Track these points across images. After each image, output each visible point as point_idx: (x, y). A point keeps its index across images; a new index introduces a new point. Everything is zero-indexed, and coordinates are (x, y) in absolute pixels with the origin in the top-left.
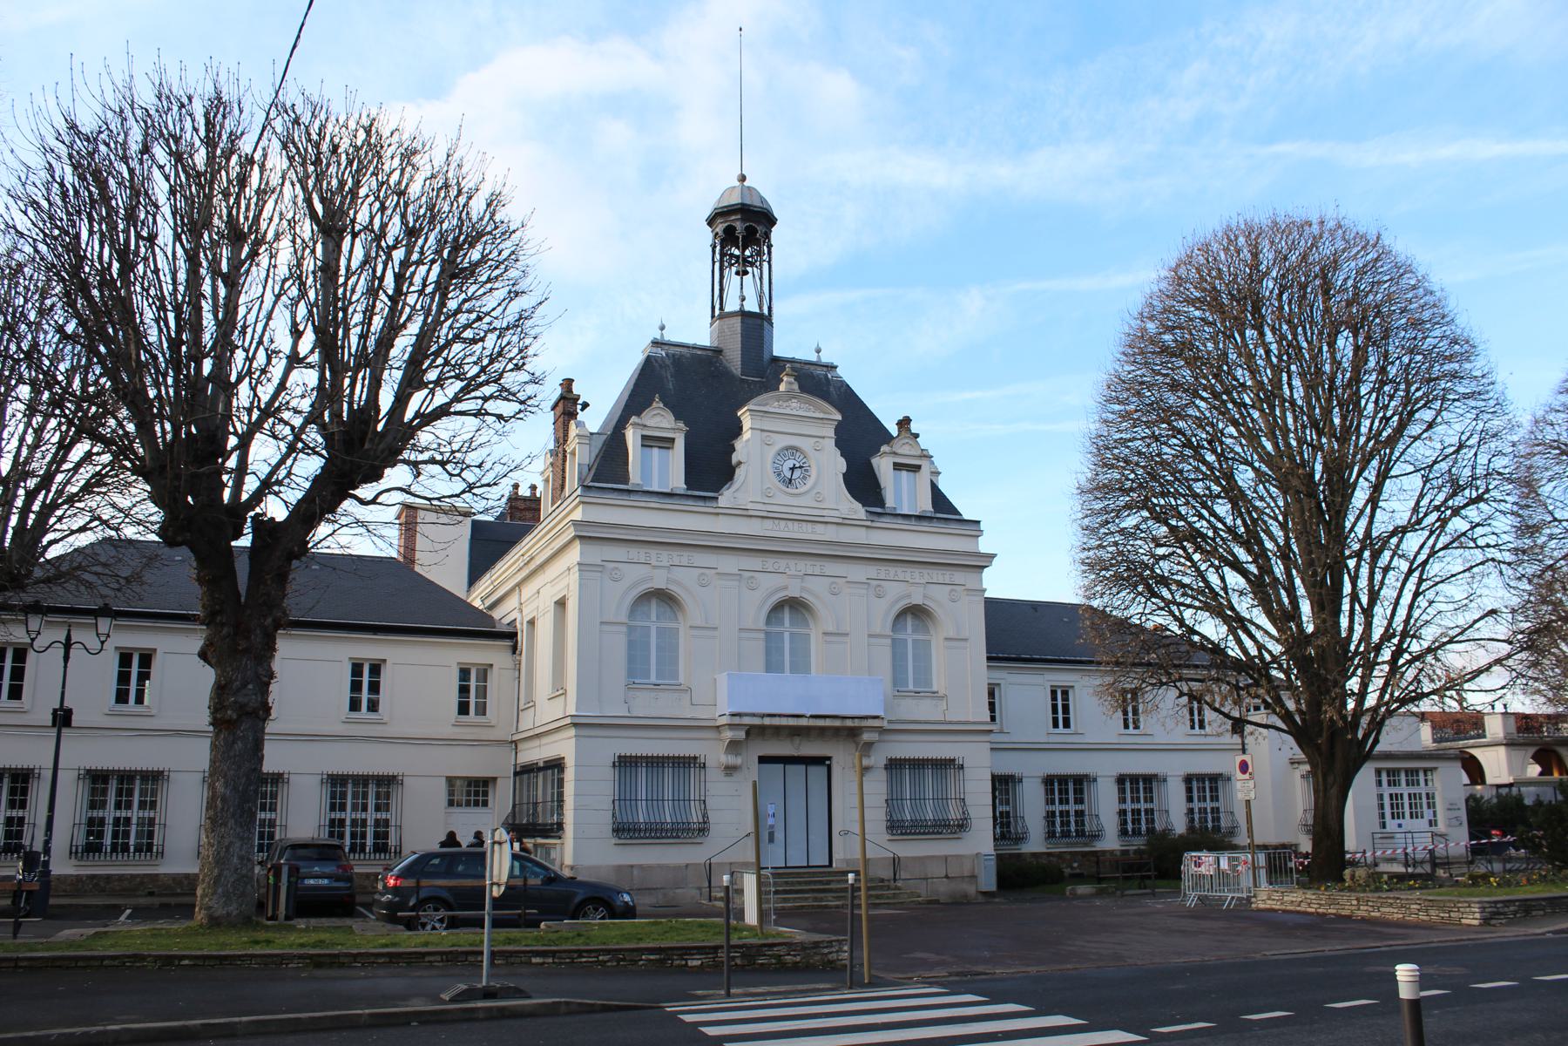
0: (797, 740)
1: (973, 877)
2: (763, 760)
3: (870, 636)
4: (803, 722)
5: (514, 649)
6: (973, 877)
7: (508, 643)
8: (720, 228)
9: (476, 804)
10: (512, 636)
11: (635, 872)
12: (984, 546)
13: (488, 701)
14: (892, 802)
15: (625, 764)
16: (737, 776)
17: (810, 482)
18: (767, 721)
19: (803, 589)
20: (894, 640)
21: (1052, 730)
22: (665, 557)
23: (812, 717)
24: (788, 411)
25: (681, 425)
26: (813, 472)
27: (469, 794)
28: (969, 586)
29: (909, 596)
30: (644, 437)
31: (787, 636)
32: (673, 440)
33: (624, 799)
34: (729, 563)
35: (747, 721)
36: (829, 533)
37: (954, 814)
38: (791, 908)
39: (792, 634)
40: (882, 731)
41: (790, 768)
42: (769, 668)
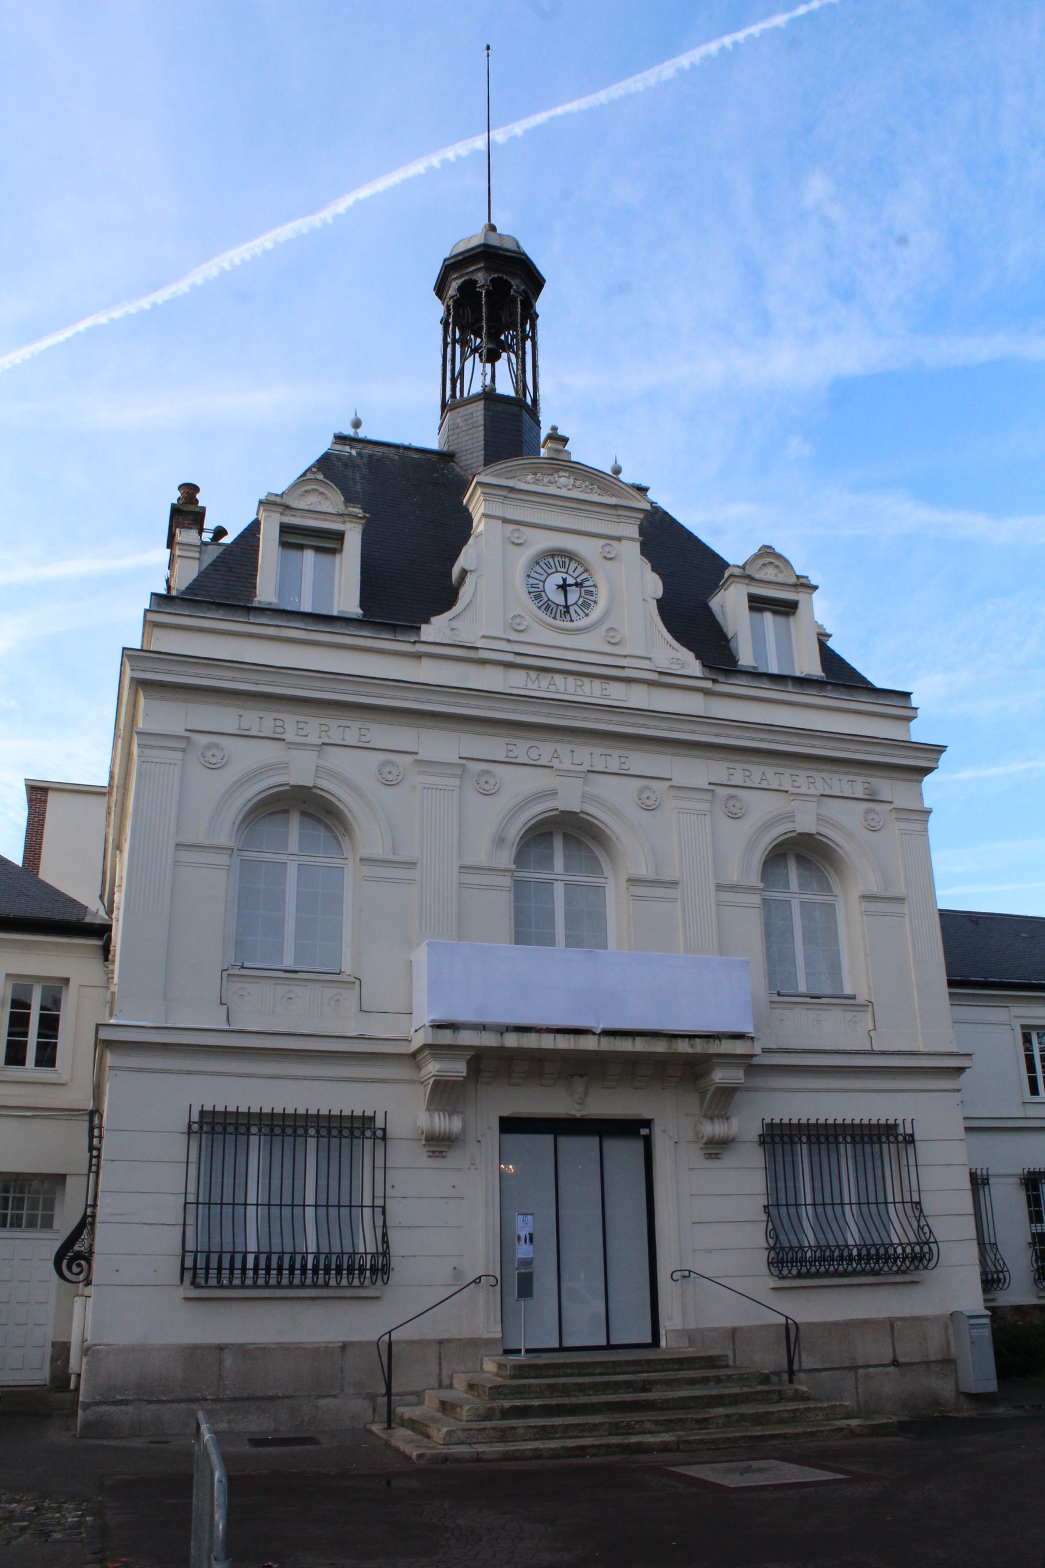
0: (579, 1085)
1: (948, 1362)
2: (510, 1125)
3: (720, 887)
4: (589, 1044)
5: (106, 952)
6: (948, 1362)
8: (452, 290)
9: (32, 1224)
10: (102, 931)
11: (228, 1362)
12: (919, 732)
13: (59, 1041)
14: (777, 1208)
15: (217, 1128)
17: (596, 613)
18: (511, 1041)
19: (585, 797)
20: (765, 901)
21: (1028, 1097)
22: (315, 727)
23: (606, 1033)
24: (552, 490)
25: (358, 511)
26: (603, 596)
28: (898, 803)
29: (790, 817)
31: (559, 889)
32: (340, 536)
33: (211, 1203)
35: (467, 1038)
36: (638, 697)
37: (899, 1232)
38: (555, 1454)
39: (567, 885)
40: (748, 1064)
41: (564, 1141)
42: (520, 938)
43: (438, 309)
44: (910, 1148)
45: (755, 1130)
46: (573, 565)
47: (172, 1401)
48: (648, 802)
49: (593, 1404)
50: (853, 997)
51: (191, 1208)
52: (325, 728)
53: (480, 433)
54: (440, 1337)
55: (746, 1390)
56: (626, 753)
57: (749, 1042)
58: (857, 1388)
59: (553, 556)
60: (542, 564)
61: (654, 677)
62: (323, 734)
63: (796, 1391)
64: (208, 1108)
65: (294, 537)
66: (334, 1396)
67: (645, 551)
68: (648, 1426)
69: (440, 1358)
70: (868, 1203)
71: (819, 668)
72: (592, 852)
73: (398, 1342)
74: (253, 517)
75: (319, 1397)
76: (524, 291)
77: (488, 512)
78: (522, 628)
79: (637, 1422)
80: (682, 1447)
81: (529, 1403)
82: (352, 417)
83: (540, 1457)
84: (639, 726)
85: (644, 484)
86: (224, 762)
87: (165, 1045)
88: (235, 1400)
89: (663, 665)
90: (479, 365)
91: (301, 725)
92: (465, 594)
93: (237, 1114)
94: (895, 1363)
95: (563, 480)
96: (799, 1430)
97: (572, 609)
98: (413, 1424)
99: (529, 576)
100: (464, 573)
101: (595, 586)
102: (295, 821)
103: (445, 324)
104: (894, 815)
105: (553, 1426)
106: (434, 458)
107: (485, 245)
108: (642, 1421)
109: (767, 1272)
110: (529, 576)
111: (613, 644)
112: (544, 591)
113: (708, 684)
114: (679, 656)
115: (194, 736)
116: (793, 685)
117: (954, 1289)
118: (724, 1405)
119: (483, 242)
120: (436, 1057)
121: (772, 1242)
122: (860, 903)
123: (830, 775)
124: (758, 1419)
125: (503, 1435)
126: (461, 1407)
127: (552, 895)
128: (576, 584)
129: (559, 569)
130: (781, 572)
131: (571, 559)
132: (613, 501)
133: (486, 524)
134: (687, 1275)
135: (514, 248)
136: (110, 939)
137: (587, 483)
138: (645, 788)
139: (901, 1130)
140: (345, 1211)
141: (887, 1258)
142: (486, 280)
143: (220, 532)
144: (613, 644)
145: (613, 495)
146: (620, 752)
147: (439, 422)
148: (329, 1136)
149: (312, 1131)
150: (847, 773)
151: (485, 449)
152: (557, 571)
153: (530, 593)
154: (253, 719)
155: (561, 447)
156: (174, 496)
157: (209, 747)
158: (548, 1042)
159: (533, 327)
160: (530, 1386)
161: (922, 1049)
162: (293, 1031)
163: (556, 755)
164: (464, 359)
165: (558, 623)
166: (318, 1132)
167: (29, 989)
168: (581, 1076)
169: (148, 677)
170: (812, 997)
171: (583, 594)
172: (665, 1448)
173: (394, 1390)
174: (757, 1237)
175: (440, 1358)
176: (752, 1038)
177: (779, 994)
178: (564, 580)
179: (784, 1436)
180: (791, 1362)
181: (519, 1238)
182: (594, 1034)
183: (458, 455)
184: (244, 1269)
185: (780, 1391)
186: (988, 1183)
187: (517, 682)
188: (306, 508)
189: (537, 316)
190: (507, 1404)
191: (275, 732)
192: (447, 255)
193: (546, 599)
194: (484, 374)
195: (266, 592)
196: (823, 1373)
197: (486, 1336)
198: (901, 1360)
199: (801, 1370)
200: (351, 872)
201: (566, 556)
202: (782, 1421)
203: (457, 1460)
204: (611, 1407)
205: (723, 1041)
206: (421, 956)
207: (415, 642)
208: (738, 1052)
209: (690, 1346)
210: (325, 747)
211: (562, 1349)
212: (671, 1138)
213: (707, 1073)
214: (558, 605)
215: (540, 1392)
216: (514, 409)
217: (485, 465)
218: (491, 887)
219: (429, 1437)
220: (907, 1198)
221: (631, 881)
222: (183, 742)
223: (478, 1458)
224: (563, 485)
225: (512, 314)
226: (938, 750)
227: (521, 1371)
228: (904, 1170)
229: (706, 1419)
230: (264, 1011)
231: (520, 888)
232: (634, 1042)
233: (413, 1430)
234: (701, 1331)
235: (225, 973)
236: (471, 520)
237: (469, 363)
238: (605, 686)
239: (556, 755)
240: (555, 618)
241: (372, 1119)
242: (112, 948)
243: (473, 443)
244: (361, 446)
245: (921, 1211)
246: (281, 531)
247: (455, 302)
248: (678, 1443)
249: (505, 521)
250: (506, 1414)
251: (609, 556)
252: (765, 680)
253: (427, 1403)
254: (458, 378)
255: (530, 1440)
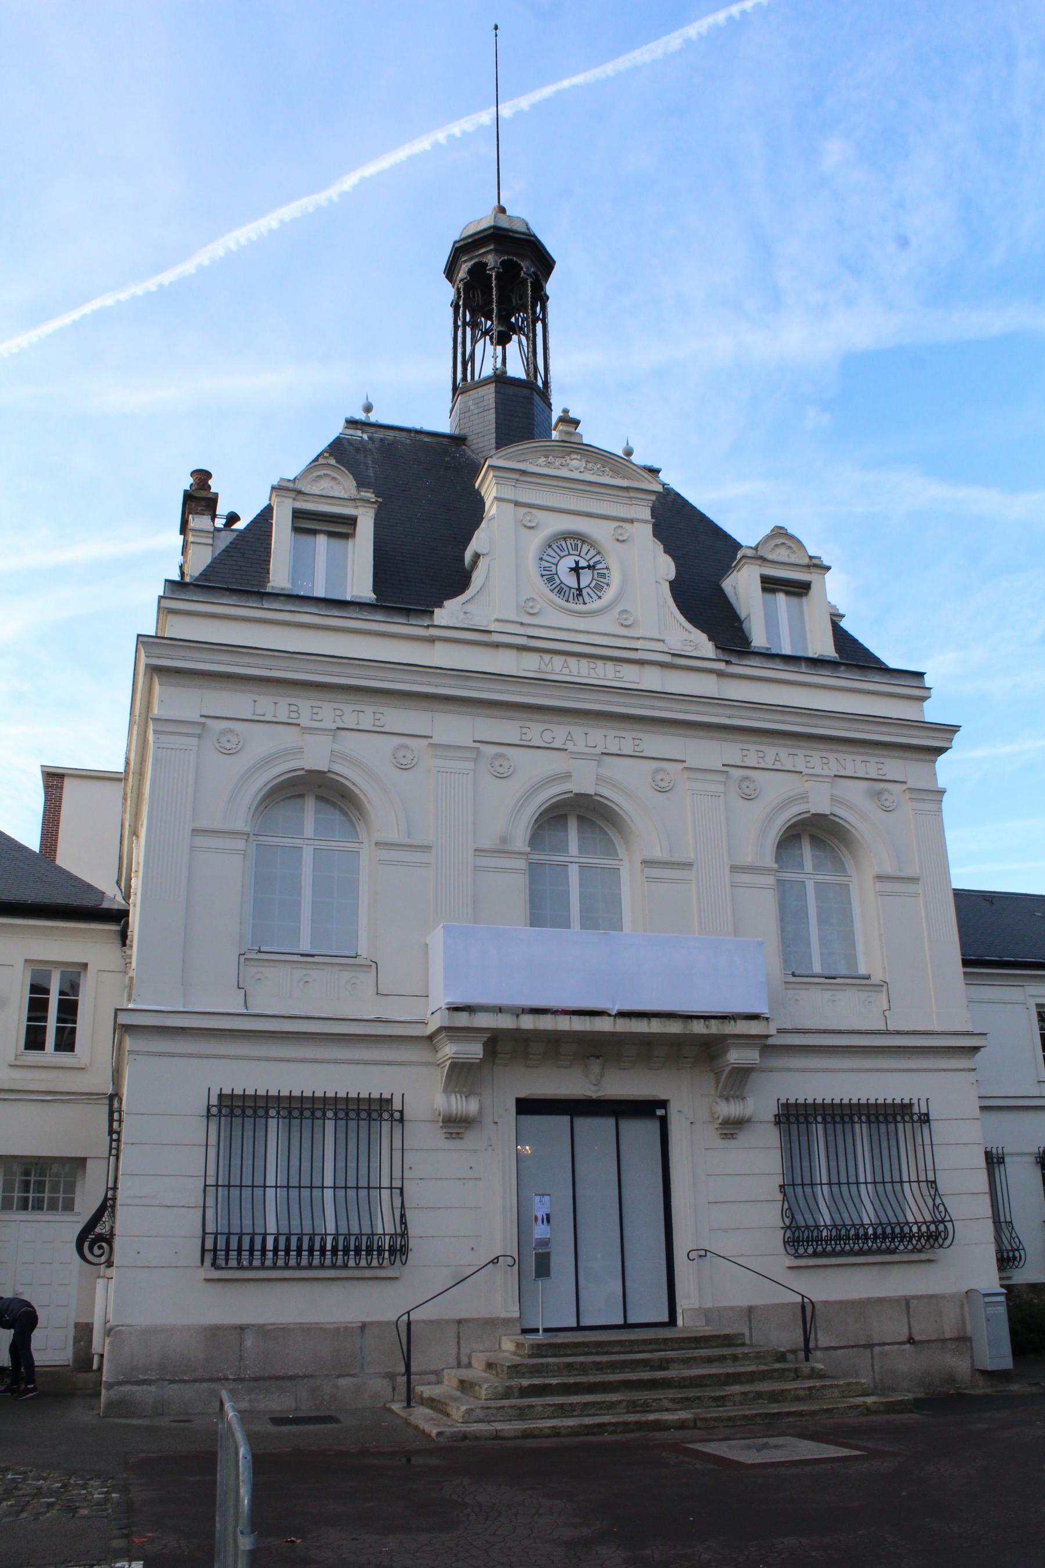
0: (595, 1067)
1: (963, 1340)
2: (526, 1107)
3: (735, 869)
4: (604, 1025)
5: (124, 937)
6: (963, 1340)
7: (115, 928)
8: (463, 272)
9: (53, 1206)
10: (120, 917)
11: (249, 1343)
12: (932, 712)
13: (78, 1026)
14: (794, 1187)
15: (235, 1111)
16: (472, 1139)
17: (609, 595)
18: (528, 1023)
19: (600, 779)
20: (780, 882)
22: (329, 712)
23: (622, 1014)
24: (564, 473)
25: (370, 495)
26: (615, 579)
27: (26, 1186)
28: (911, 784)
29: (804, 797)
30: (298, 515)
31: (574, 871)
32: (352, 521)
33: (230, 1185)
34: (455, 728)
35: (484, 1021)
36: (651, 679)
37: (915, 1212)
38: (573, 1432)
40: (764, 1045)
42: (536, 920)
43: (448, 292)
44: (925, 1127)
45: (771, 1110)
46: (585, 548)
47: (194, 1381)
48: (662, 784)
49: (610, 1383)
50: (868, 978)
51: (211, 1191)
52: (339, 713)
53: (492, 416)
54: (457, 1318)
55: (763, 1368)
56: (640, 735)
57: (764, 1023)
58: (873, 1366)
59: (565, 539)
60: (554, 546)
61: (667, 659)
62: (338, 718)
63: (813, 1369)
64: (227, 1091)
65: (306, 523)
66: (353, 1375)
67: (658, 532)
68: (666, 1404)
69: (459, 1338)
70: (884, 1183)
71: (833, 648)
72: (606, 834)
73: (416, 1321)
74: (265, 503)
75: (339, 1376)
76: (534, 273)
77: (499, 496)
78: (535, 611)
79: (654, 1400)
80: (699, 1424)
81: (547, 1381)
82: (362, 402)
83: (558, 1435)
84: (653, 708)
85: (656, 466)
86: (239, 747)
87: (183, 1029)
88: (256, 1379)
89: (676, 647)
90: (490, 348)
91: (315, 710)
92: (478, 578)
93: (313, 1099)
94: (911, 1341)
95: (574, 462)
96: (815, 1407)
97: (584, 592)
98: (431, 1403)
99: (541, 559)
100: (477, 556)
101: (607, 568)
102: (310, 805)
103: (456, 307)
104: (908, 795)
105: (571, 1404)
106: (445, 441)
107: (495, 227)
108: (660, 1399)
109: (783, 1251)
110: (541, 559)
111: (626, 626)
112: (556, 574)
113: (721, 666)
114: (692, 637)
115: (209, 722)
116: (806, 666)
117: (968, 1269)
118: (741, 1383)
119: (492, 223)
120: (451, 1039)
121: (787, 1222)
122: (875, 884)
123: (844, 756)
124: (774, 1397)
125: (522, 1414)
126: (480, 1386)
127: (567, 878)
128: (589, 567)
129: (572, 552)
130: (794, 552)
131: (583, 542)
132: (625, 483)
133: (498, 507)
134: (704, 1253)
135: (524, 229)
136: (127, 924)
137: (599, 466)
138: (658, 771)
139: (916, 1110)
140: (363, 1193)
141: (903, 1237)
142: (496, 262)
143: (233, 518)
144: (626, 626)
145: (624, 477)
146: (634, 735)
147: (451, 405)
148: (347, 1118)
149: (330, 1114)
150: (862, 754)
151: (496, 432)
152: (569, 554)
153: (542, 576)
154: (268, 704)
155: (572, 430)
156: (187, 482)
157: (224, 732)
158: (564, 1024)
159: (544, 309)
160: (548, 1364)
161: (937, 1029)
162: (310, 1014)
163: (570, 738)
164: (474, 341)
165: (571, 606)
166: (336, 1114)
167: (48, 975)
168: (597, 1057)
169: (162, 664)
170: (826, 978)
171: (596, 577)
172: (682, 1425)
173: (413, 1369)
174: (771, 1217)
175: (459, 1338)
176: (767, 1019)
177: (794, 975)
178: (577, 563)
179: (801, 1414)
180: (807, 1340)
181: (536, 1219)
182: (610, 1015)
183: (469, 438)
184: (264, 1250)
185: (796, 1370)
186: (1003, 1162)
187: (529, 665)
188: (319, 493)
189: (548, 298)
190: (525, 1382)
191: (289, 717)
192: (457, 238)
193: (558, 582)
194: (495, 357)
195: (279, 577)
196: (839, 1352)
197: (504, 1315)
198: (917, 1338)
199: (817, 1348)
200: (366, 855)
201: (578, 539)
202: (798, 1399)
203: (477, 1438)
204: (628, 1385)
205: (739, 1022)
206: (437, 939)
207: (428, 626)
208: (753, 1032)
209: (707, 1325)
210: (339, 732)
211: (579, 1328)
212: (687, 1119)
213: (725, 1051)
214: (570, 588)
215: (559, 1370)
216: (525, 392)
217: (497, 448)
218: (504, 870)
219: (448, 1415)
220: (922, 1178)
221: (647, 863)
222: (199, 728)
223: (497, 1436)
224: (575, 467)
225: (523, 296)
226: (952, 730)
227: (539, 1350)
228: (920, 1149)
229: (723, 1397)
230: (281, 994)
231: (535, 870)
232: (649, 1023)
233: (432, 1408)
234: (718, 1310)
235: (242, 958)
236: (483, 504)
237: (479, 346)
238: (618, 668)
239: (570, 738)
240: (567, 601)
241: (390, 1101)
242: (129, 933)
243: (483, 427)
244: (373, 430)
245: (936, 1190)
246: (294, 517)
247: (465, 285)
248: (695, 1421)
249: (517, 504)
250: (525, 1392)
251: (621, 538)
252: (778, 660)
253: (446, 1382)
254: (468, 361)
255: (548, 1418)
